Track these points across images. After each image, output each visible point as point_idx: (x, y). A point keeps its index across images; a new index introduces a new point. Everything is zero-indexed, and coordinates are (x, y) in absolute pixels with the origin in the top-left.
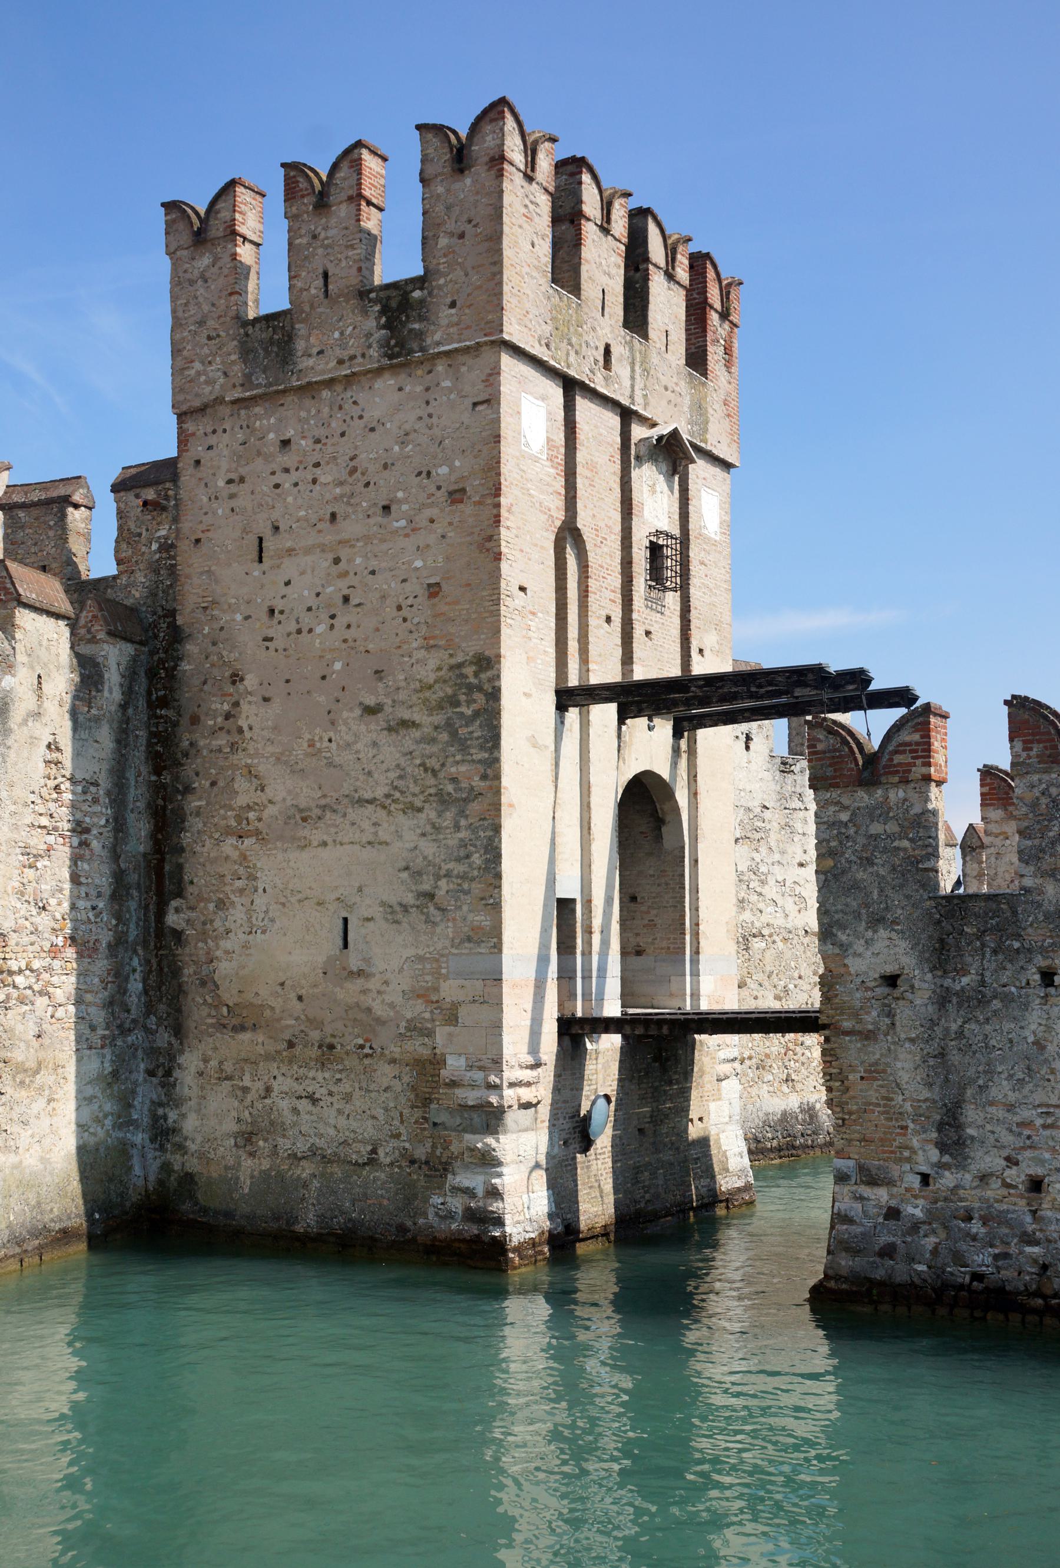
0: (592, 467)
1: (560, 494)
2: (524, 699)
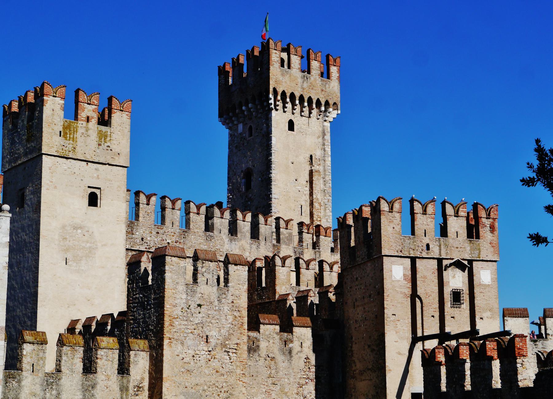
0: (425, 277)
2: (395, 343)
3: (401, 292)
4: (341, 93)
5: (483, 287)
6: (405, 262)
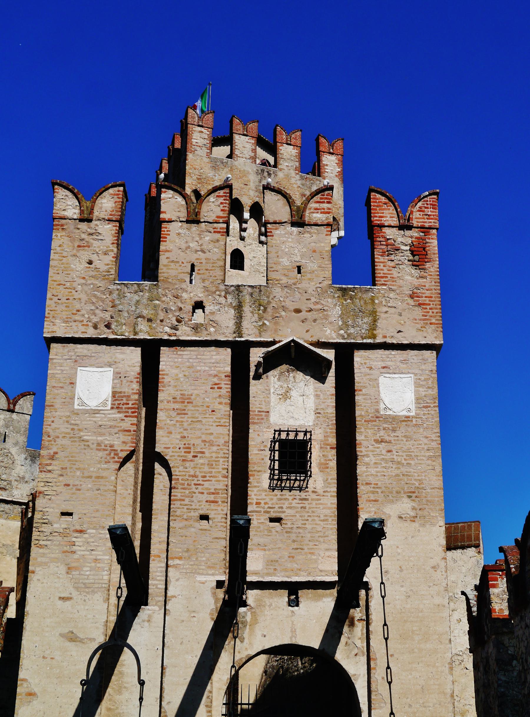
1: (130, 431)
2: (60, 602)
3: (99, 444)
4: (345, 201)
5: (385, 426)
6: (120, 356)
